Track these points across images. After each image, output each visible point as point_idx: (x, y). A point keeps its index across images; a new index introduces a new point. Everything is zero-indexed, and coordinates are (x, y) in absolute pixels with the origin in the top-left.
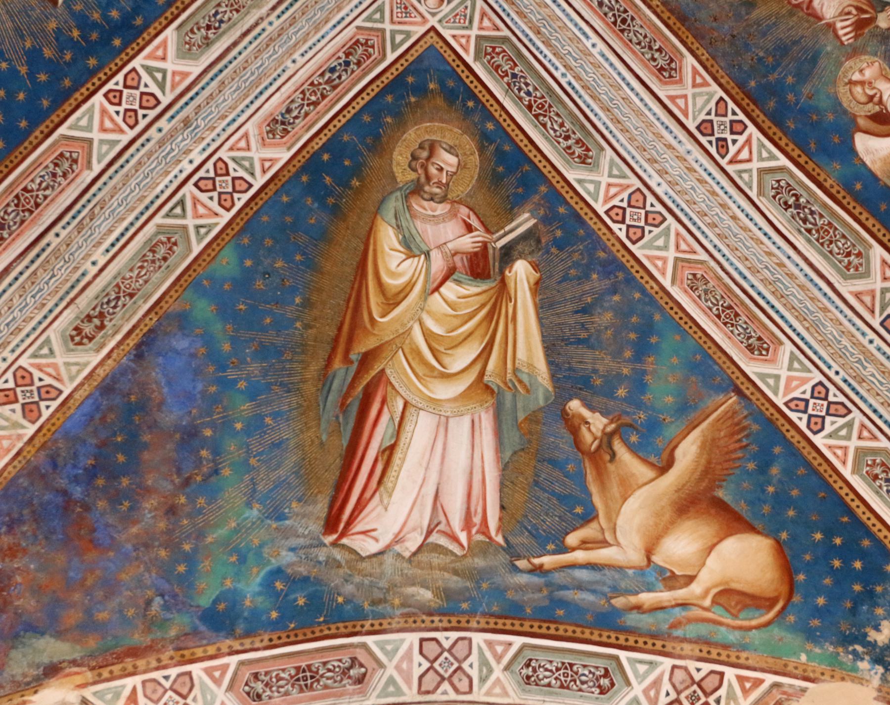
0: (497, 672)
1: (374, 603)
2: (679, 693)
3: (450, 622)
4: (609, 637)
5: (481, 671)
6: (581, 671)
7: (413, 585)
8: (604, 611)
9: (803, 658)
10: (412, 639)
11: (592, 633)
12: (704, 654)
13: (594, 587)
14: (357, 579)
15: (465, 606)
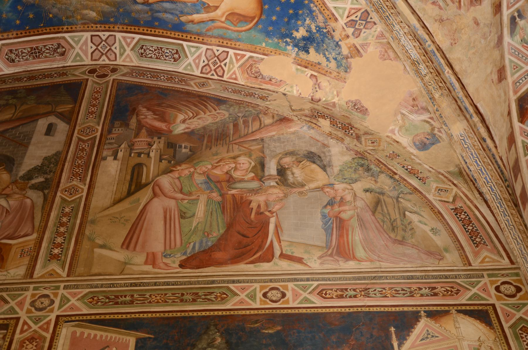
0: (128, 51)
1: (67, 18)
2: (209, 61)
3: (105, 27)
4: (179, 35)
5: (120, 51)
6: (166, 51)
7: (87, 9)
8: (176, 23)
9: (264, 45)
10: (88, 35)
11: (171, 34)
12: (221, 43)
13: (172, 12)
14: (59, 6)
15: (112, 20)
